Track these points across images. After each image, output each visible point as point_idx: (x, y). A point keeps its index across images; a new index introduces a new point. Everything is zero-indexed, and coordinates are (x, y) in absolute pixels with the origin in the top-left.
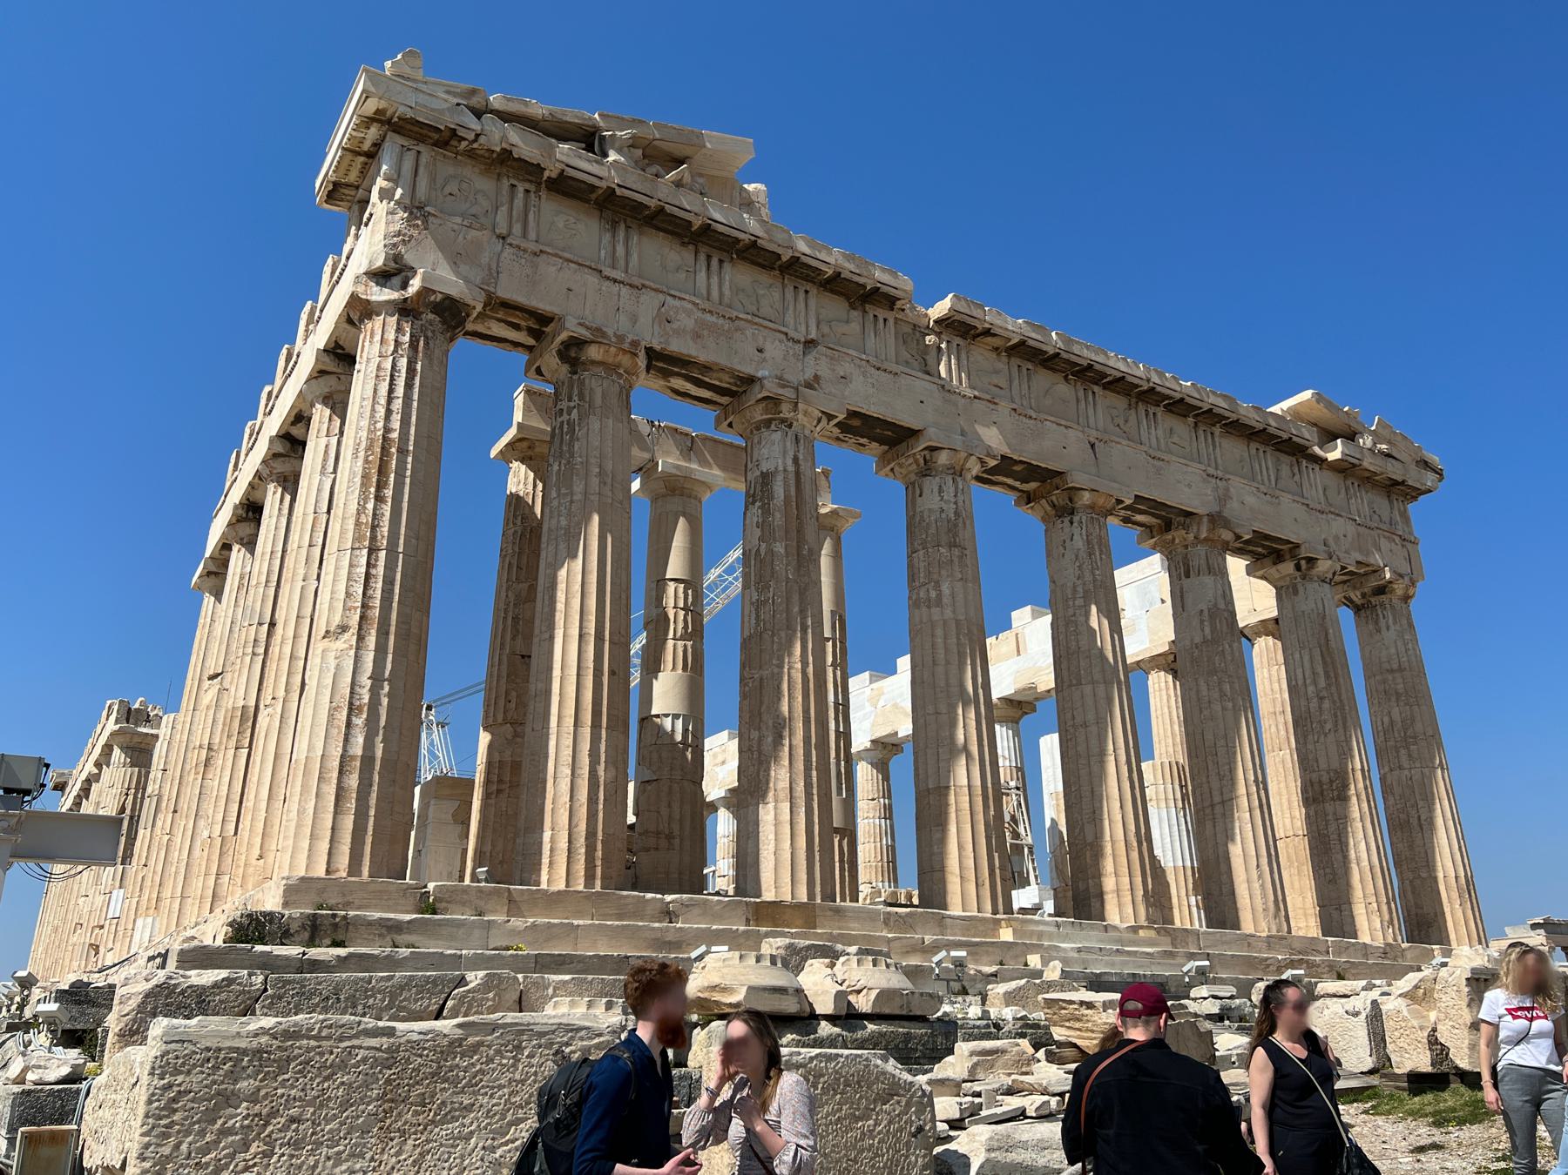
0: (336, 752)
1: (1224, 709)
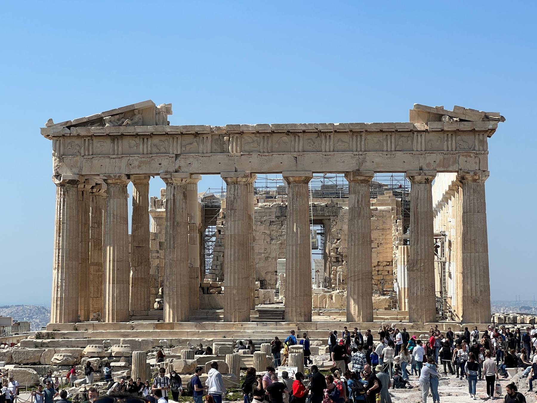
0: (56, 297)
1: (351, 245)
